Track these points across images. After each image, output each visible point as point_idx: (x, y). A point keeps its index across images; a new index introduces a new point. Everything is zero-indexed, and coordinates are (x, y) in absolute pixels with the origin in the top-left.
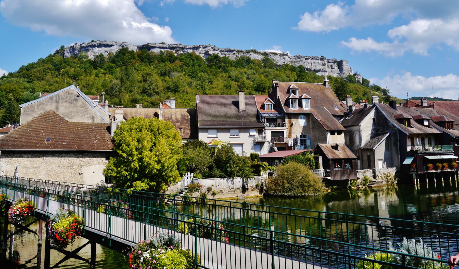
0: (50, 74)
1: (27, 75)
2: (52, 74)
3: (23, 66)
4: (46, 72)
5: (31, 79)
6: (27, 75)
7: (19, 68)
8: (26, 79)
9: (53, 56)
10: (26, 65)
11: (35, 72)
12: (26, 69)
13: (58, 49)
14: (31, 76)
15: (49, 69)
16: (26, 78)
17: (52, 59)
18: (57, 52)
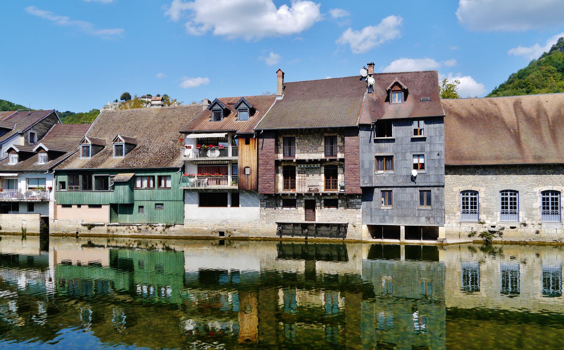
0: (552, 77)
1: (524, 84)
2: (554, 77)
3: (513, 74)
4: (546, 76)
5: (529, 88)
6: (524, 84)
7: (508, 77)
8: (524, 89)
9: (550, 54)
10: (517, 72)
11: (533, 79)
12: (518, 77)
13: (556, 44)
14: (529, 84)
15: (549, 71)
16: (523, 87)
17: (550, 58)
18: (554, 49)
